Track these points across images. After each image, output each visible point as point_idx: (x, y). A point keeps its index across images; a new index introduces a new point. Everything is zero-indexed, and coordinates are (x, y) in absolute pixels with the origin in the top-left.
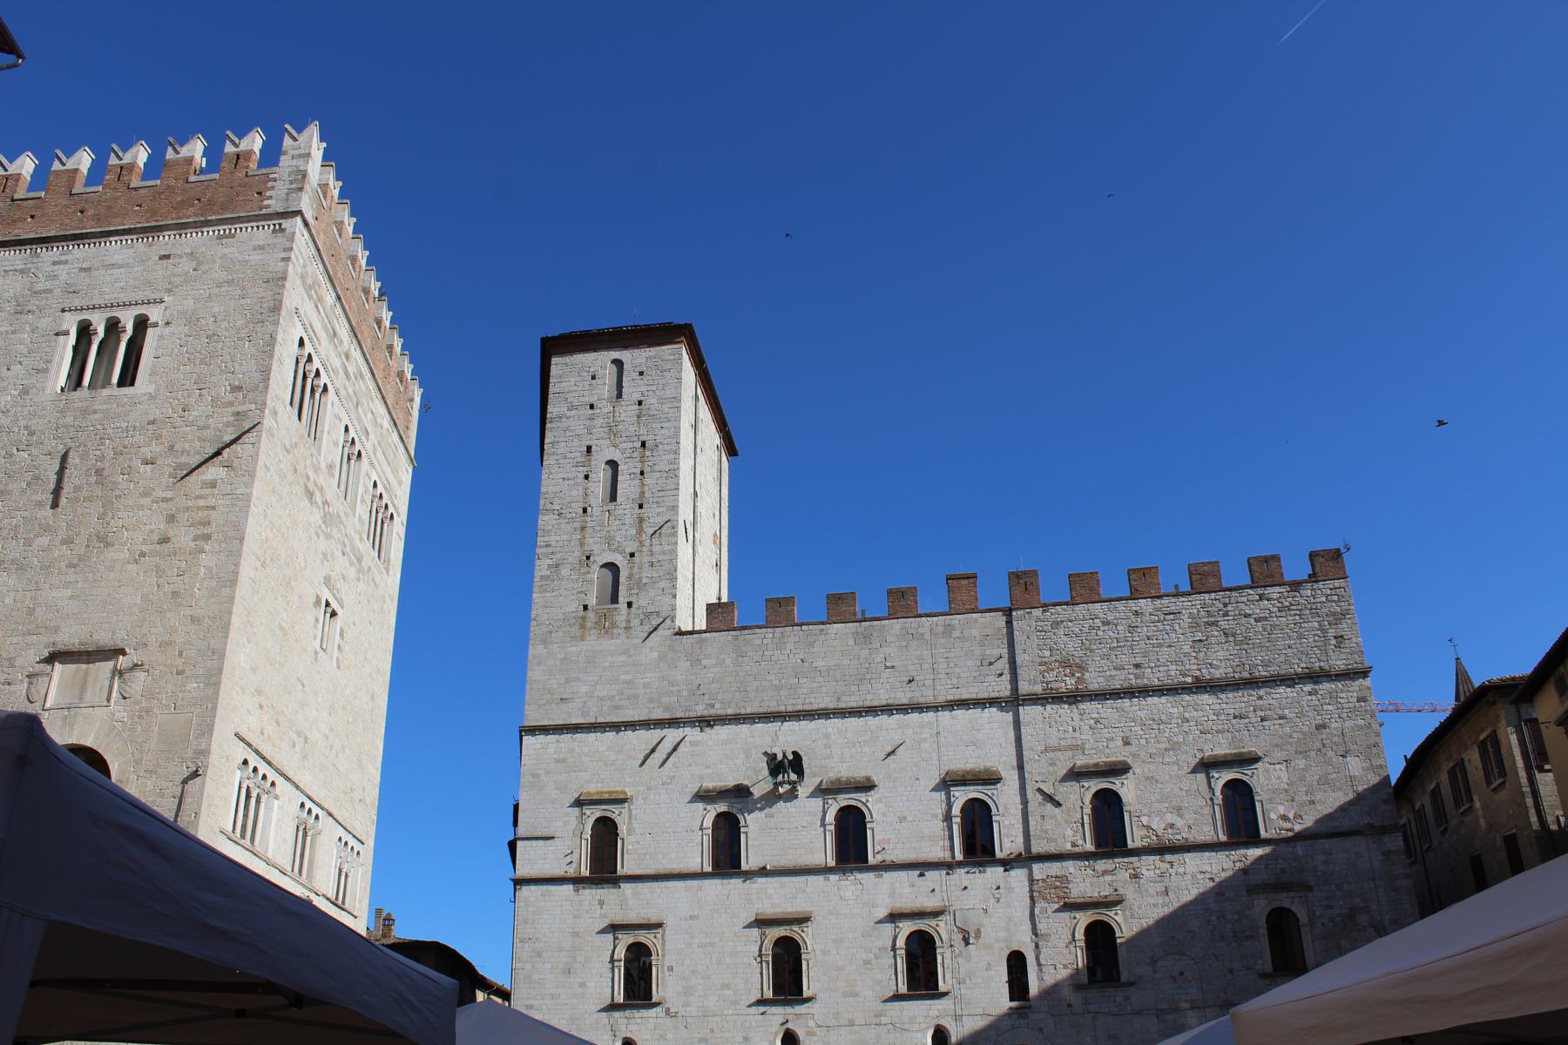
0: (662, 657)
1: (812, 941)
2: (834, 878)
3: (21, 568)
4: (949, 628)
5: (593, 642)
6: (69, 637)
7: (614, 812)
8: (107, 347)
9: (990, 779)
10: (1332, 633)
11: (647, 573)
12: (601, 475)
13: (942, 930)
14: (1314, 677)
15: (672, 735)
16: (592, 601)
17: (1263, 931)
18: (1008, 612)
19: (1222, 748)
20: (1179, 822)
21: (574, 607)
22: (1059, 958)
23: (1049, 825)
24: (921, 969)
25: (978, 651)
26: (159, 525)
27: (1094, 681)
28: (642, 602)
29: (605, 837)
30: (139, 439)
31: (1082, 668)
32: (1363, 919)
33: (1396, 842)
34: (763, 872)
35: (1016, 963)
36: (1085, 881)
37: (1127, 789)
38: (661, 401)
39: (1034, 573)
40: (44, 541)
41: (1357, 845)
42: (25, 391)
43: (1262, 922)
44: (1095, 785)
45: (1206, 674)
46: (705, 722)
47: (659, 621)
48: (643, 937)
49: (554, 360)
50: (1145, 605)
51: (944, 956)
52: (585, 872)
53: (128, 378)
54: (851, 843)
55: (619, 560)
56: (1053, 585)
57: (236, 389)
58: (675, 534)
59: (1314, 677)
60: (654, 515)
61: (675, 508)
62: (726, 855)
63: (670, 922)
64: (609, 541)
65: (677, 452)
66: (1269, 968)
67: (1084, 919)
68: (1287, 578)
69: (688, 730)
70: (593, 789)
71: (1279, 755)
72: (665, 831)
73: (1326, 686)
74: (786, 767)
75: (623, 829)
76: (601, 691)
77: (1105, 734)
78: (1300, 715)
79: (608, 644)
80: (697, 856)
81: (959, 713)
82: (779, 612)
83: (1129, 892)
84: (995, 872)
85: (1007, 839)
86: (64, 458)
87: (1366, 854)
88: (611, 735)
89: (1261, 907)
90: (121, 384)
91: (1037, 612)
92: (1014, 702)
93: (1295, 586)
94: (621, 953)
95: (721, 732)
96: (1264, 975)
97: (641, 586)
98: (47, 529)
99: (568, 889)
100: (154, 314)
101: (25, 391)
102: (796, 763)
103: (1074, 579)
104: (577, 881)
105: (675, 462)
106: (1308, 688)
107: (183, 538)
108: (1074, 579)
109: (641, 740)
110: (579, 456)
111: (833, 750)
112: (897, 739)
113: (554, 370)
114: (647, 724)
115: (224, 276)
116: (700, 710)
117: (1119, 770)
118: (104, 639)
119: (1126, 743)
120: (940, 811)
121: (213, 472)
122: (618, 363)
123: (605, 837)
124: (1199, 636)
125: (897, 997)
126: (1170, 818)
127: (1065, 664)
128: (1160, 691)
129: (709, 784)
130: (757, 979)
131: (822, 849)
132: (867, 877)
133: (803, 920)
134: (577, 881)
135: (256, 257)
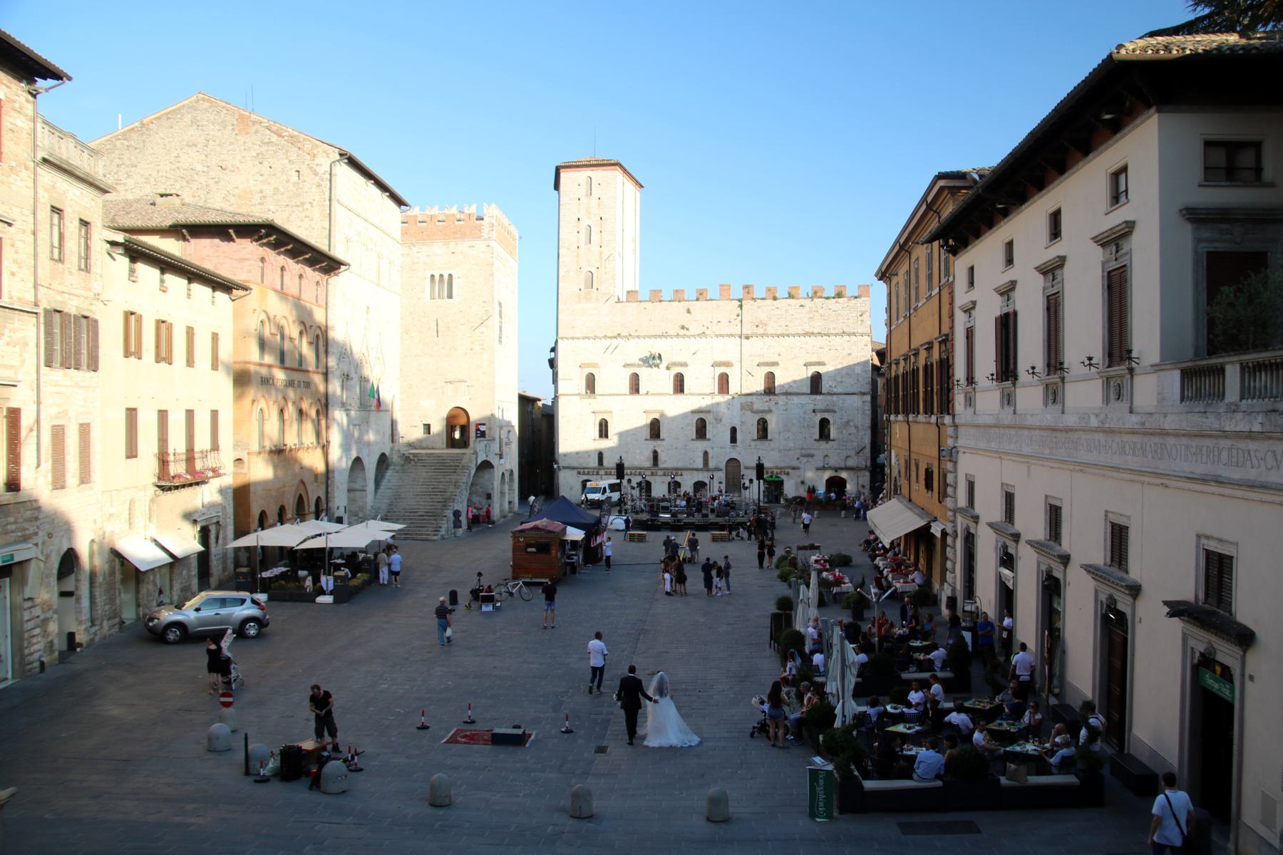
9: (728, 364)
13: (708, 418)
15: (615, 342)
18: (740, 300)
19: (814, 359)
22: (748, 431)
24: (701, 430)
27: (770, 331)
33: (868, 398)
35: (734, 430)
36: (759, 404)
52: (583, 391)
53: (450, 296)
56: (759, 292)
62: (635, 387)
66: (817, 436)
67: (757, 417)
72: (613, 379)
80: (625, 386)
82: (656, 296)
83: (773, 408)
89: (819, 417)
103: (769, 290)
108: (769, 290)
111: (672, 350)
114: (605, 337)
117: (775, 364)
120: (711, 375)
121: (482, 329)
130: (647, 433)
131: (669, 386)
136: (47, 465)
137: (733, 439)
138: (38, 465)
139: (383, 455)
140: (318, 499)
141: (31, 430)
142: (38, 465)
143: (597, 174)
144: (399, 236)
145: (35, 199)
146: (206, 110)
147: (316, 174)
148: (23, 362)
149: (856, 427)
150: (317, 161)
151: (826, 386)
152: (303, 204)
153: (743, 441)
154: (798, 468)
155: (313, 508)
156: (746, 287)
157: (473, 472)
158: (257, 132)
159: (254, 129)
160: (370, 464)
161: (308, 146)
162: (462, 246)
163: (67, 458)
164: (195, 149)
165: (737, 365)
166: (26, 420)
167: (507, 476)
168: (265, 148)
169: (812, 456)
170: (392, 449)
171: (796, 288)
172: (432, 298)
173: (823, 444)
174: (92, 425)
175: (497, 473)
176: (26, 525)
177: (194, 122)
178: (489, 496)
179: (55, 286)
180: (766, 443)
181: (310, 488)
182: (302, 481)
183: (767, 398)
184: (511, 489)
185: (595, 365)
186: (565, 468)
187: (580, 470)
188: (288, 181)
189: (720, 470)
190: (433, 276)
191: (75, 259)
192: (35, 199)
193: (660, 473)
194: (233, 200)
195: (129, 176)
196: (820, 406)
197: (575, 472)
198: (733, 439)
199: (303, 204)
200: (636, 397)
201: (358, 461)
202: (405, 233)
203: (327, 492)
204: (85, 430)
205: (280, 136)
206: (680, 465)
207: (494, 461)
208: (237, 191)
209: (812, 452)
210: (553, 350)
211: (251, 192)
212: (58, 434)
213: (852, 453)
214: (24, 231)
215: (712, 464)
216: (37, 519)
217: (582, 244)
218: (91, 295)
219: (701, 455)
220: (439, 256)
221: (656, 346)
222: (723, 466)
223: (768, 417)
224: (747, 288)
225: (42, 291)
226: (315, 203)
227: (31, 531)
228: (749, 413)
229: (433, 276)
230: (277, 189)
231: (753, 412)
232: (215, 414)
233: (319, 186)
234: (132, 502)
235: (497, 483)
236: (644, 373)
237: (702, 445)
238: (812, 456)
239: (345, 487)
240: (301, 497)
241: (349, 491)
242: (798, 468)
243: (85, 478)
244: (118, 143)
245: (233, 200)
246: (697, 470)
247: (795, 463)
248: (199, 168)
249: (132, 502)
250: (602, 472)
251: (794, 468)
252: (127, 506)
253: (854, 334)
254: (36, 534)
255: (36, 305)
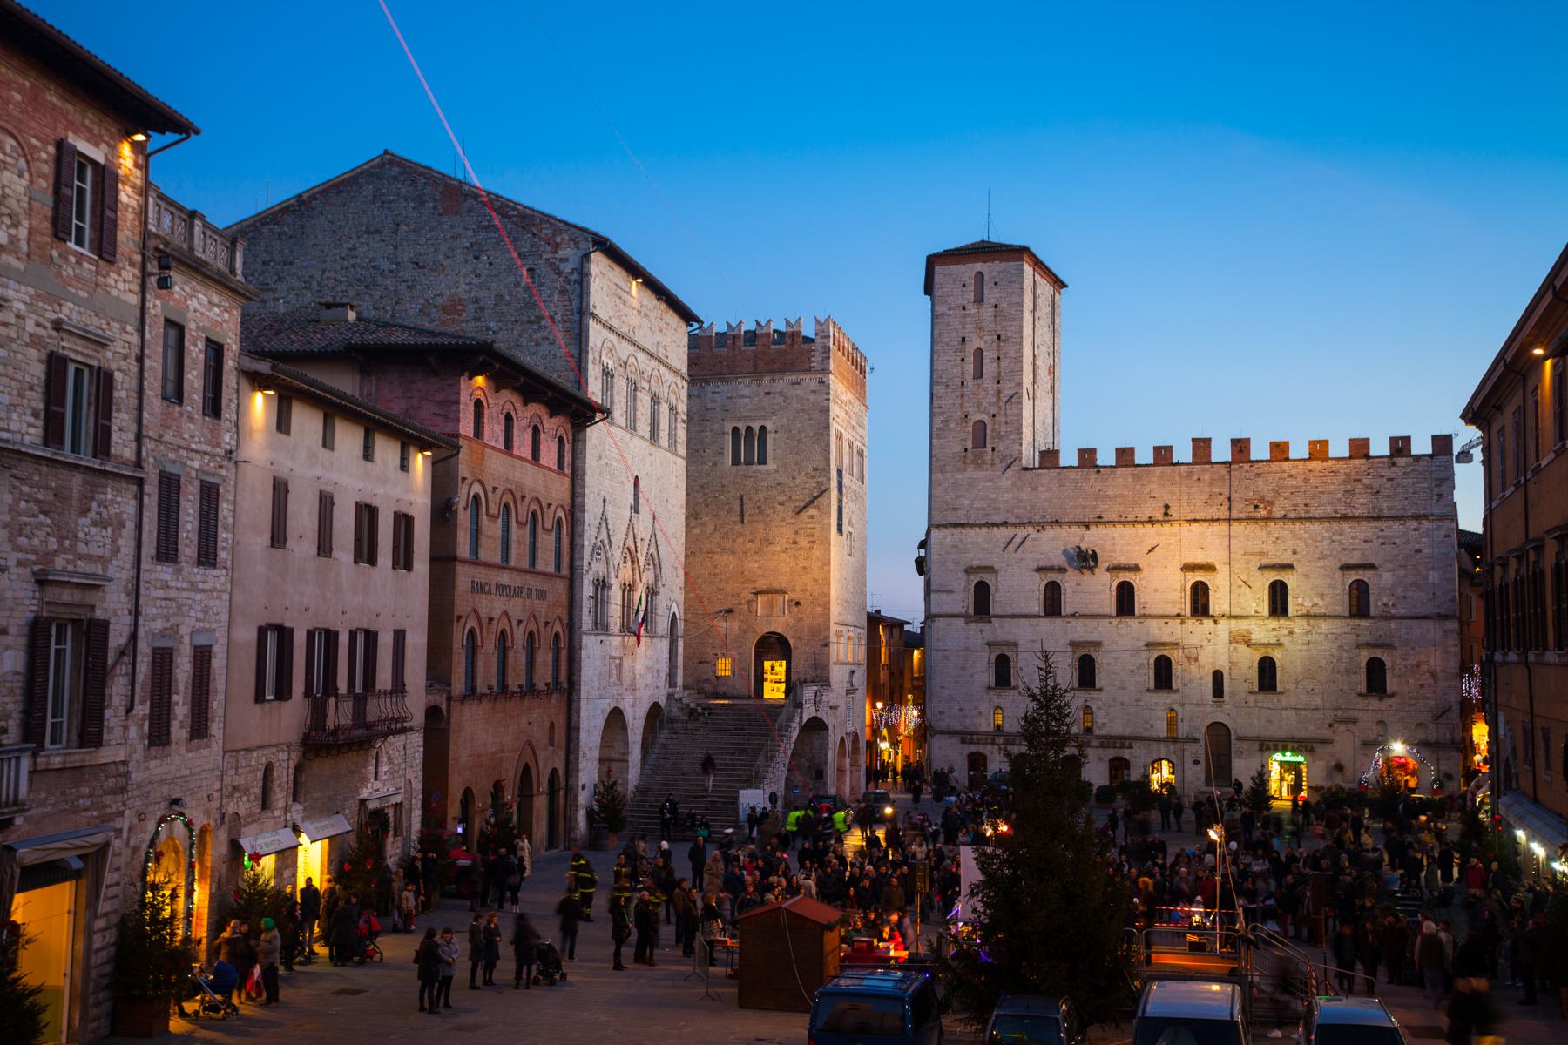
0: (1014, 484)
1: (1101, 659)
2: (1115, 621)
3: (733, 552)
4: (1190, 474)
5: (971, 472)
6: (761, 584)
7: (987, 578)
8: (749, 446)
9: (1209, 568)
10: (1436, 491)
11: (1003, 429)
12: (970, 359)
13: (1176, 656)
14: (1417, 517)
15: (1022, 533)
16: (970, 446)
17: (1364, 670)
19: (1355, 559)
20: (1321, 603)
21: (958, 449)
23: (1242, 599)
25: (1207, 489)
26: (790, 535)
28: (1001, 447)
29: (982, 594)
30: (774, 492)
31: (1271, 503)
32: (1424, 668)
33: (1455, 625)
34: (1073, 615)
35: (1218, 677)
37: (1291, 580)
38: (1010, 305)
39: (1248, 440)
40: (740, 540)
41: (1431, 623)
42: (715, 464)
43: (1363, 665)
44: (1273, 576)
45: (1350, 512)
46: (1041, 526)
47: (1012, 460)
48: (1005, 650)
49: (937, 269)
50: (1316, 464)
51: (1176, 670)
52: (971, 611)
53: (762, 461)
54: (1126, 600)
55: (985, 418)
57: (815, 469)
58: (1020, 403)
59: (1417, 517)
60: (1007, 389)
61: (1020, 384)
62: (1053, 602)
63: (1022, 643)
64: (979, 405)
65: (1021, 344)
66: (1364, 690)
67: (1258, 656)
68: (1414, 452)
69: (1030, 529)
70: (975, 563)
71: (1390, 566)
73: (1426, 524)
74: (1086, 560)
75: (992, 588)
76: (977, 505)
77: (1283, 546)
78: (1408, 542)
79: (980, 474)
81: (1195, 526)
83: (1285, 641)
84: (1208, 623)
85: (1218, 603)
86: (741, 498)
87: (1433, 630)
88: (984, 530)
89: (1364, 656)
90: (760, 463)
91: (1247, 466)
92: (1229, 520)
93: (1418, 458)
94: (993, 659)
95: (1051, 532)
96: (1360, 695)
97: (1000, 437)
98: (741, 534)
99: (962, 621)
100: (769, 427)
101: (715, 464)
102: (1094, 556)
104: (965, 616)
105: (1020, 350)
106: (1414, 524)
107: (803, 542)
109: (1003, 534)
110: (956, 343)
112: (1155, 543)
113: (937, 278)
114: (1005, 523)
115: (798, 406)
116: (1037, 518)
117: (1290, 567)
118: (776, 585)
119: (1295, 553)
121: (812, 511)
122: (980, 276)
123: (982, 594)
124: (1349, 488)
125: (1148, 690)
126: (1316, 600)
127: (1262, 500)
128: (1320, 519)
129: (1042, 564)
131: (1111, 608)
132: (1133, 622)
133: (1098, 644)
134: (965, 616)
135: (812, 397)
136: (142, 710)
137: (1218, 691)
138: (129, 709)
139: (655, 705)
140: (554, 772)
141: (122, 653)
142: (129, 709)
143: (991, 269)
144: (684, 370)
145: (143, 309)
146: (395, 178)
147: (559, 274)
148: (116, 551)
149: (1434, 675)
150: (561, 253)
151: (1376, 603)
152: (539, 318)
153: (1233, 694)
154: (1330, 742)
155: (545, 786)
156: (1234, 442)
157: (795, 735)
158: (470, 211)
159: (466, 205)
160: (636, 720)
161: (547, 231)
162: (782, 383)
163: (175, 698)
164: (377, 237)
165: (1223, 570)
166: (117, 639)
167: (848, 743)
168: (482, 235)
169: (1355, 721)
170: (670, 696)
171: (1325, 443)
172: (736, 461)
173: (1374, 703)
174: (215, 649)
175: (833, 739)
176: (108, 799)
177: (377, 196)
178: (820, 775)
179: (167, 437)
180: (1275, 698)
181: (541, 754)
182: (530, 744)
183: (1273, 623)
184: (855, 763)
185: (990, 569)
186: (942, 732)
187: (966, 736)
188: (517, 284)
189: (1196, 740)
190: (735, 430)
191: (197, 398)
192: (143, 309)
193: (1095, 743)
194: (434, 313)
195: (279, 279)
196: (1366, 638)
197: (955, 740)
198: (1218, 691)
199: (539, 318)
200: (1058, 621)
201: (616, 716)
202: (693, 362)
203: (568, 762)
204: (202, 656)
205: (505, 215)
206: (1127, 732)
207: (829, 721)
208: (440, 300)
209: (1355, 714)
210: (922, 545)
211: (461, 302)
212: (163, 660)
213: (1425, 717)
214: (125, 357)
215: (1183, 730)
216: (123, 790)
217: (969, 376)
218: (221, 452)
219: (1164, 715)
220: (746, 398)
221: (1093, 539)
222: (1201, 733)
223: (1277, 655)
224: (1240, 447)
225: (148, 445)
226: (558, 317)
227: (114, 809)
228: (1243, 648)
229: (735, 430)
230: (500, 297)
231: (1249, 644)
232: (400, 635)
233: (563, 292)
234: (269, 769)
235: (832, 755)
236: (1070, 582)
237: (1163, 699)
238: (1355, 721)
239: (596, 754)
240: (527, 767)
241: (602, 760)
242: (1330, 742)
243: (199, 728)
244: (265, 230)
245: (434, 313)
246: (1158, 740)
247: (1327, 733)
248: (385, 265)
249: (269, 769)
250: (1001, 740)
251: (1323, 742)
252: (260, 774)
253: (1425, 516)
254: (121, 814)
255: (138, 463)
